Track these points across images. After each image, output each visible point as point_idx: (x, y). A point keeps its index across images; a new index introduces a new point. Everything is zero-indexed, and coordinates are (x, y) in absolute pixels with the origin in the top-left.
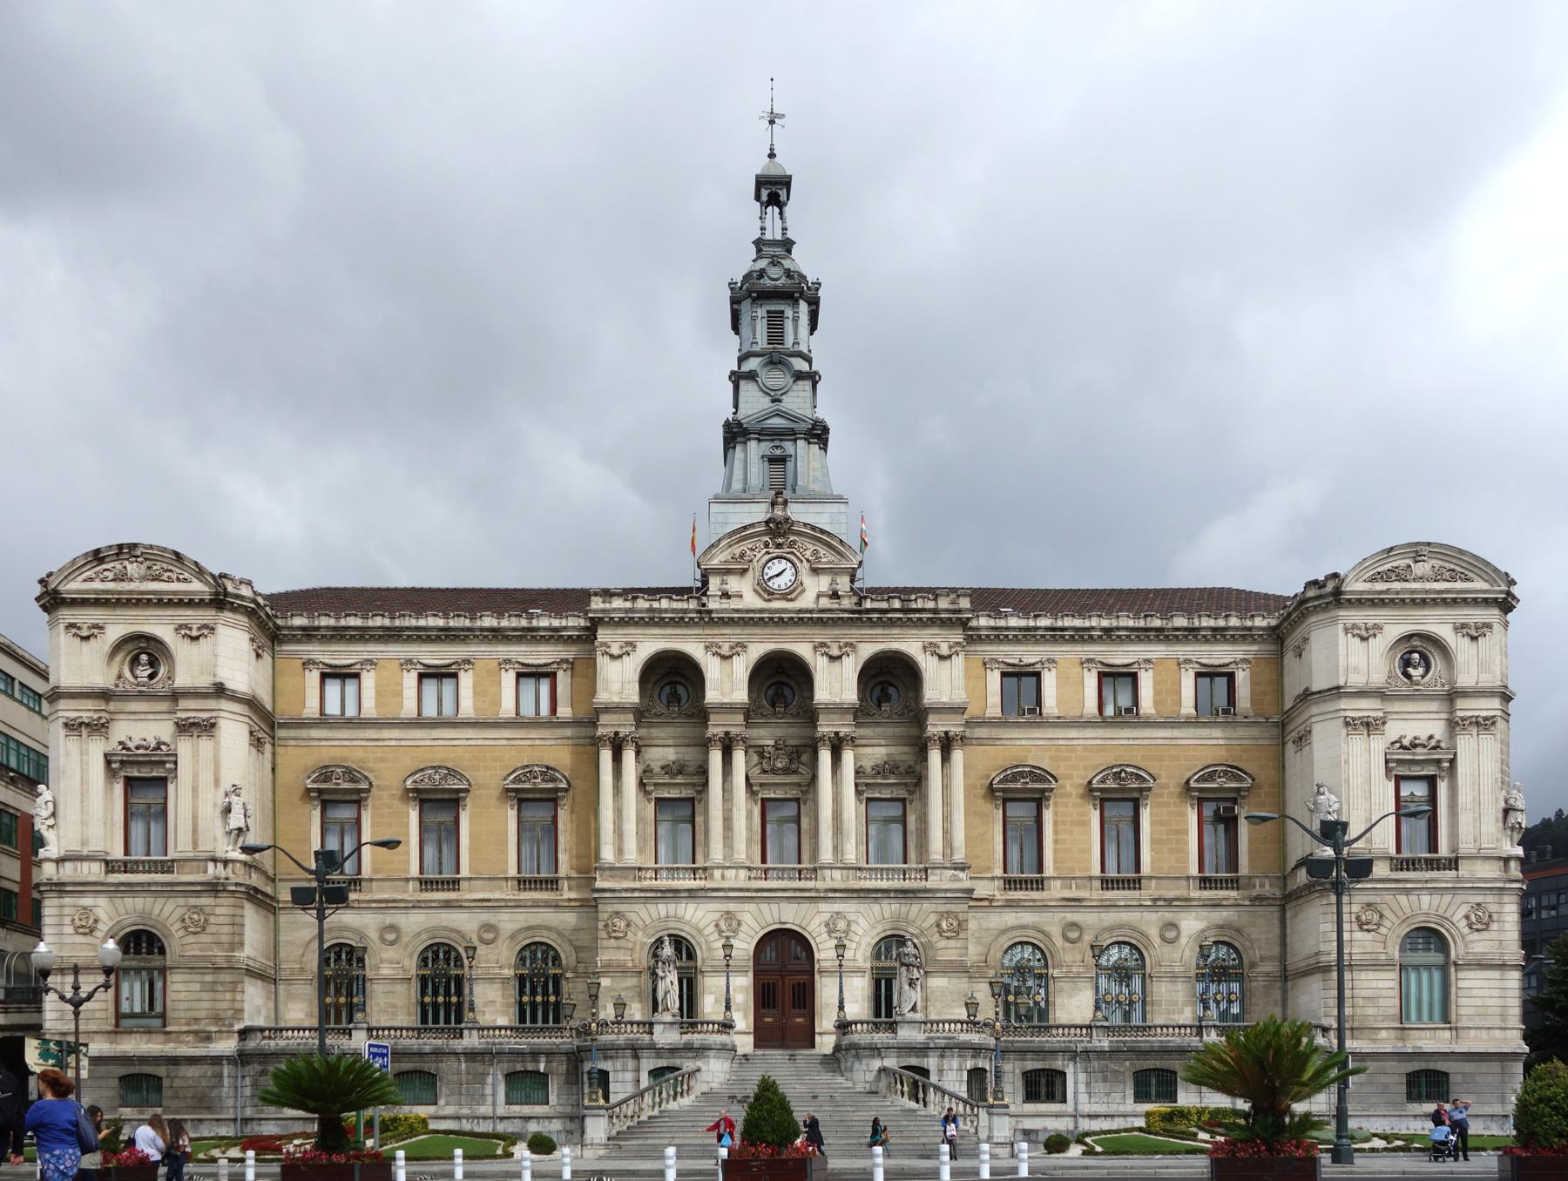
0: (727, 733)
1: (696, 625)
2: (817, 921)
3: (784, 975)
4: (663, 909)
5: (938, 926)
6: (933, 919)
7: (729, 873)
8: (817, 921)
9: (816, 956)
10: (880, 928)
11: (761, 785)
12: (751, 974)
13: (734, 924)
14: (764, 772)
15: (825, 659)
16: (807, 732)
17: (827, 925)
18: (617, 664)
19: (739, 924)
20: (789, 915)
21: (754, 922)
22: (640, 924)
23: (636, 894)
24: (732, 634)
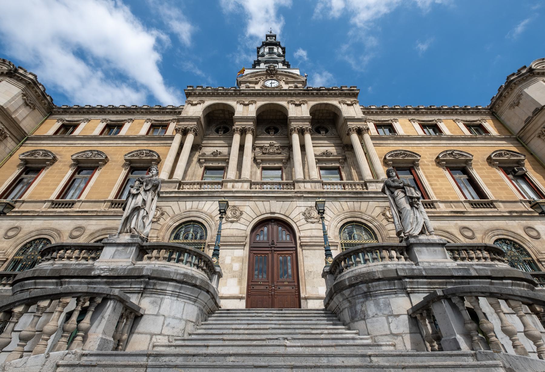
0: (243, 128)
1: (234, 96)
2: (297, 211)
3: (273, 246)
4: (189, 205)
5: (384, 214)
6: (378, 211)
7: (237, 185)
8: (297, 211)
9: (298, 235)
10: (342, 217)
11: (262, 160)
12: (247, 248)
13: (238, 213)
14: (264, 154)
15: (293, 106)
16: (286, 142)
17: (304, 214)
18: (194, 107)
19: (241, 213)
20: (278, 208)
21: (252, 211)
22: (171, 213)
23: (173, 195)
24: (250, 99)
